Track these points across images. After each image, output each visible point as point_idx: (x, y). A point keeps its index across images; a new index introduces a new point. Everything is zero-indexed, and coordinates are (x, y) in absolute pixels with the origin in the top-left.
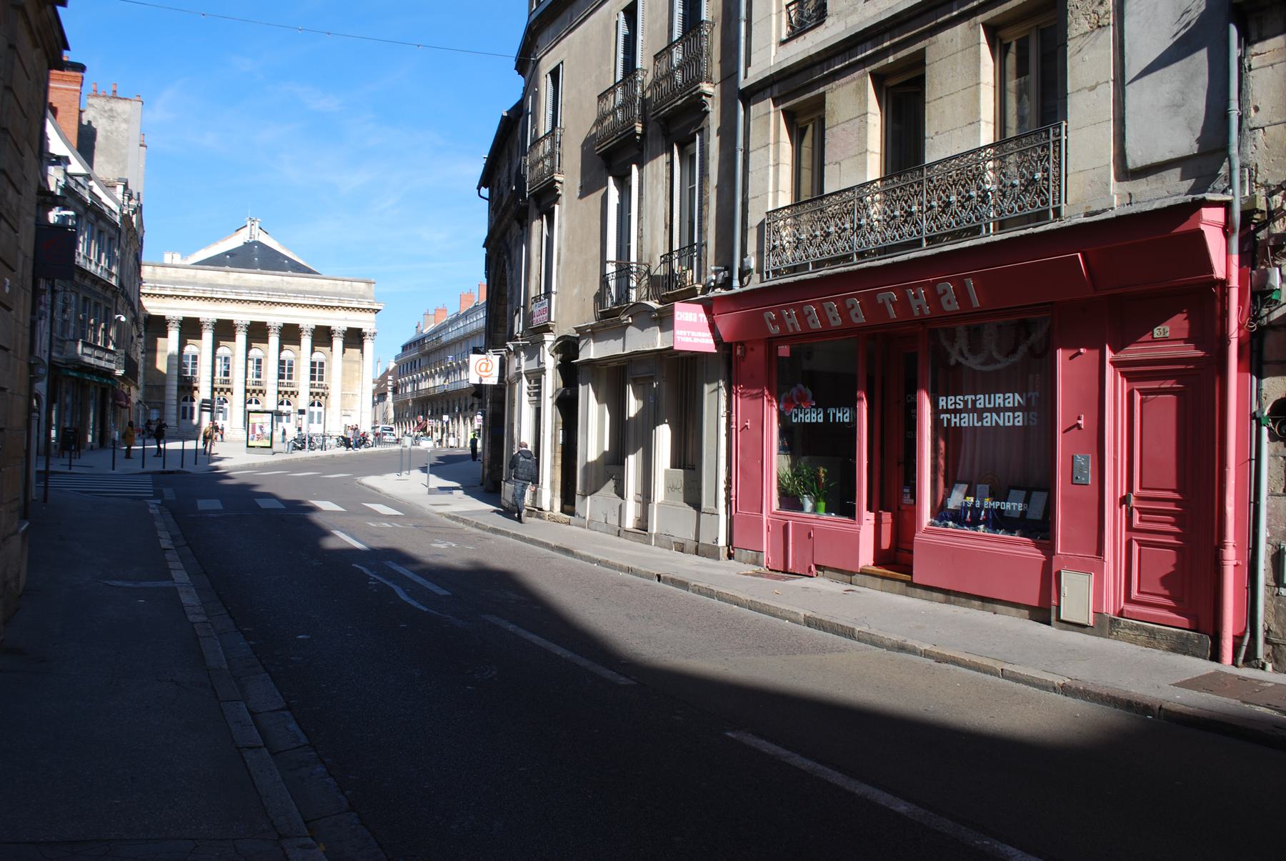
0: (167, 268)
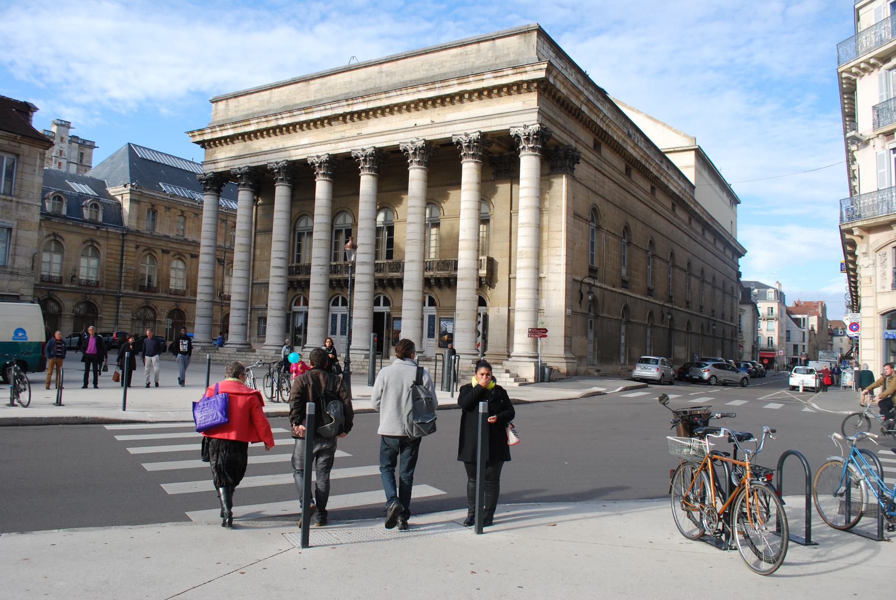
0: (241, 99)
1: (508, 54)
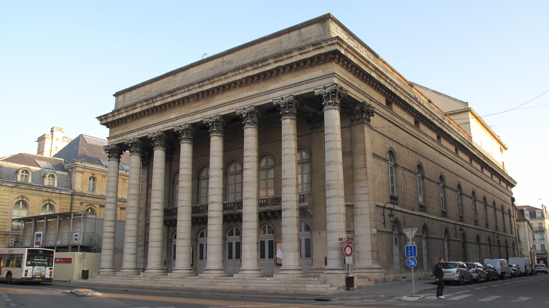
1: (311, 38)
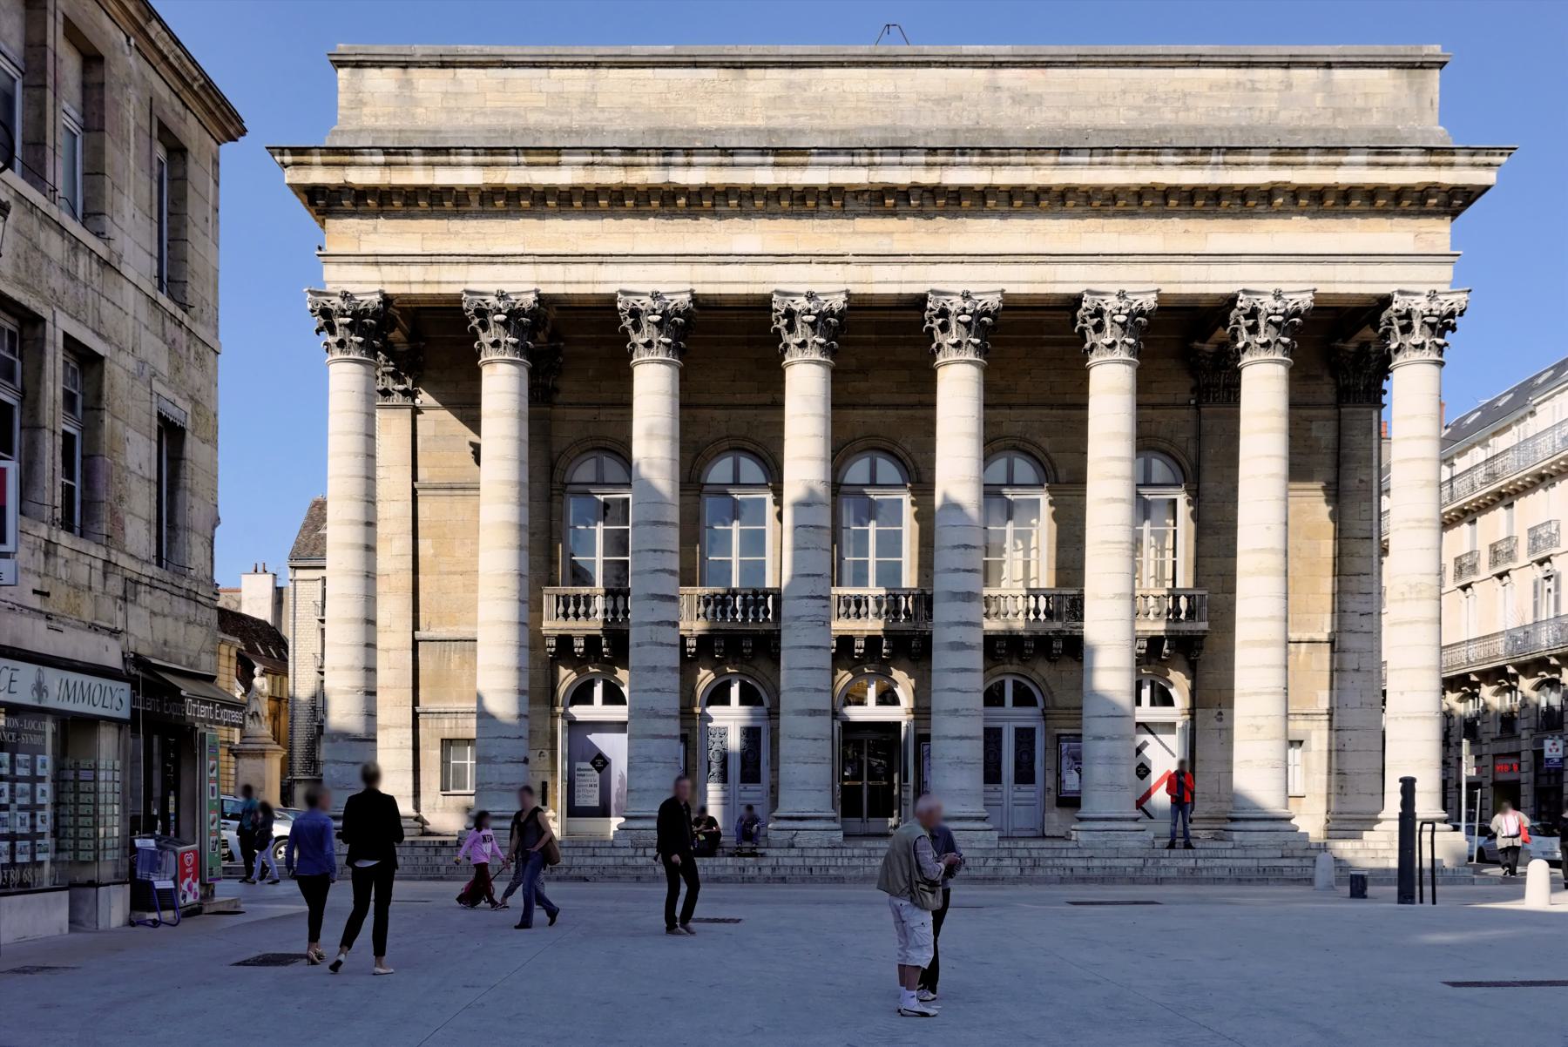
0: (462, 72)
1: (1365, 111)
